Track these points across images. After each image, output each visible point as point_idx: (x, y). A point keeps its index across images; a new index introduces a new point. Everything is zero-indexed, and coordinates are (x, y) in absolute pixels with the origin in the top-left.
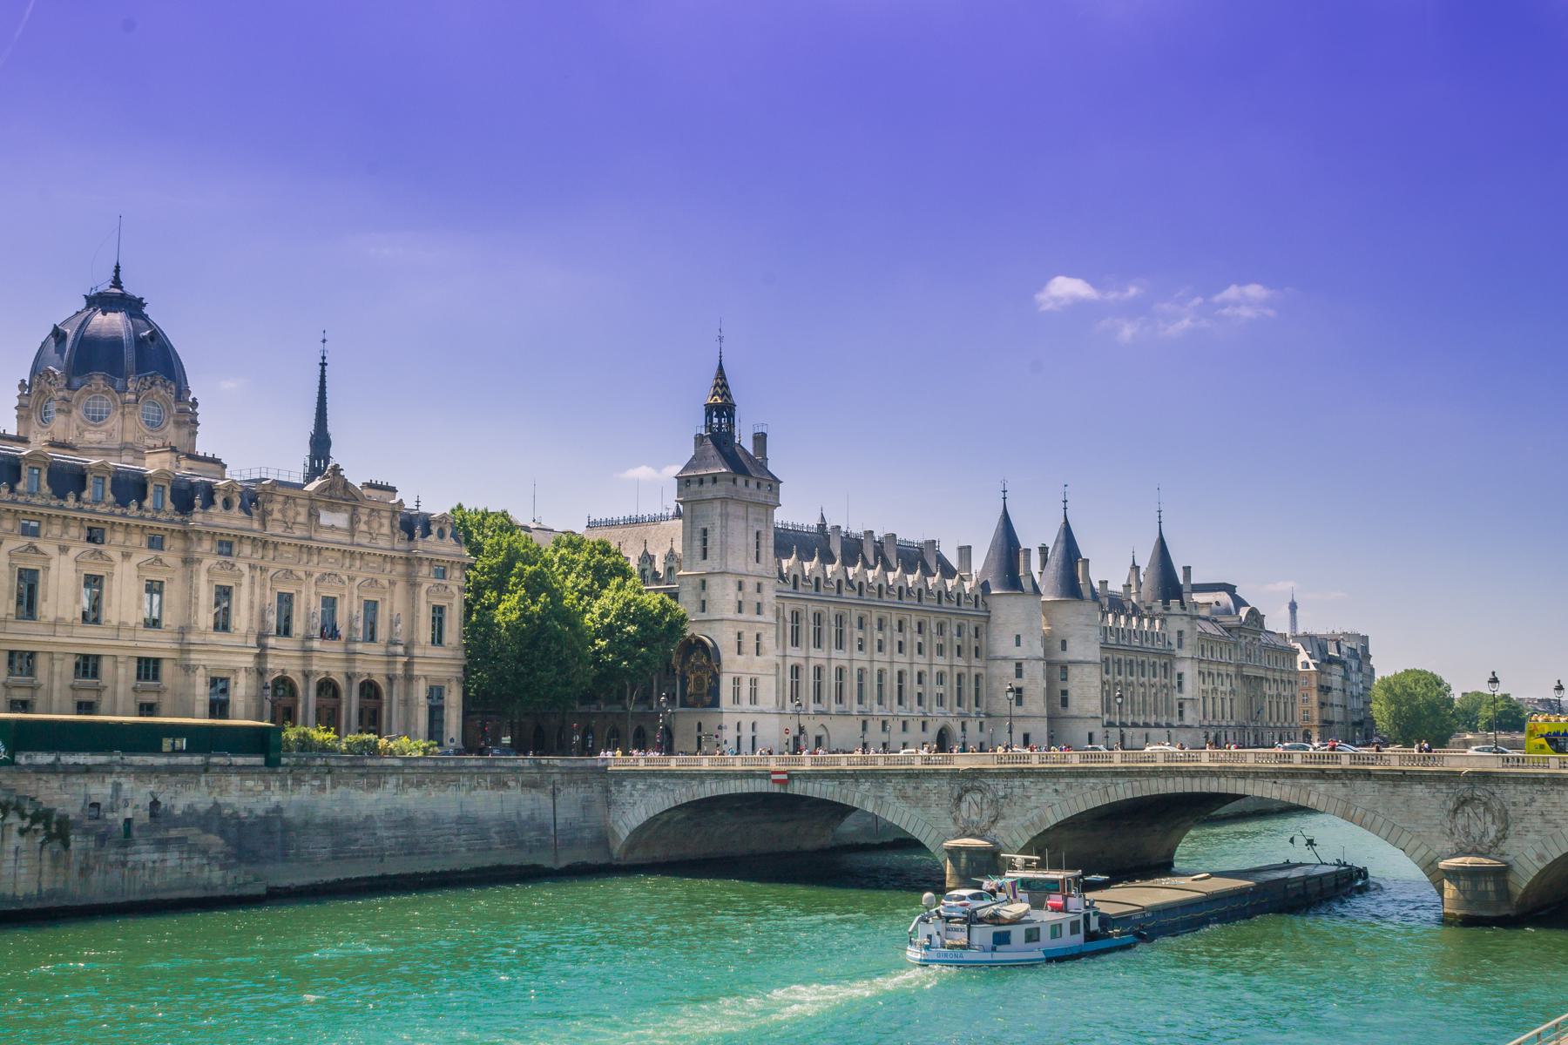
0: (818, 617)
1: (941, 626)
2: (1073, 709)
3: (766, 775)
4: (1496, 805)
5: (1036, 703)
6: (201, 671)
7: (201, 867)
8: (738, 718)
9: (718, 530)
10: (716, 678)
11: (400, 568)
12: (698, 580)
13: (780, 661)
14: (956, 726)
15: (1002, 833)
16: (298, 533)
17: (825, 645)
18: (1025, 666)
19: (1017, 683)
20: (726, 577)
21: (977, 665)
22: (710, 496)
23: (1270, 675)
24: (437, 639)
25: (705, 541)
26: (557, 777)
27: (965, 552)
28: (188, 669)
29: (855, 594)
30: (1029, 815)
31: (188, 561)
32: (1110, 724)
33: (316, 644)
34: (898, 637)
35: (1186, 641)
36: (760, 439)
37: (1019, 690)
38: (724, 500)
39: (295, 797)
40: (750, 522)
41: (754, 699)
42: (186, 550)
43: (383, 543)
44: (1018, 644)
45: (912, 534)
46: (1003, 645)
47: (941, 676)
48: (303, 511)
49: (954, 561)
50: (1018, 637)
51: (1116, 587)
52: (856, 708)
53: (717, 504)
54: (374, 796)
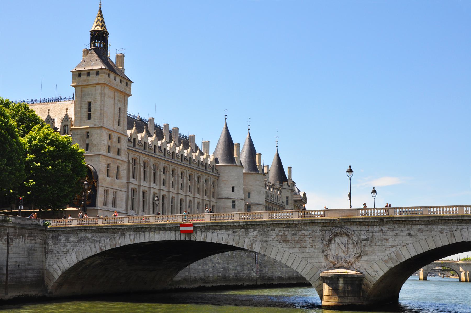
1: (199, 178)
3: (175, 228)
9: (98, 103)
12: (84, 132)
13: (126, 184)
15: (365, 266)
17: (148, 179)
18: (236, 202)
20: (103, 130)
22: (94, 82)
25: (89, 110)
26: (11, 230)
29: (162, 155)
30: (387, 252)
34: (181, 182)
36: (121, 58)
38: (103, 85)
40: (116, 102)
41: (114, 205)
44: (233, 191)
45: (185, 132)
46: (226, 191)
47: (198, 203)
50: (233, 188)
53: (99, 87)
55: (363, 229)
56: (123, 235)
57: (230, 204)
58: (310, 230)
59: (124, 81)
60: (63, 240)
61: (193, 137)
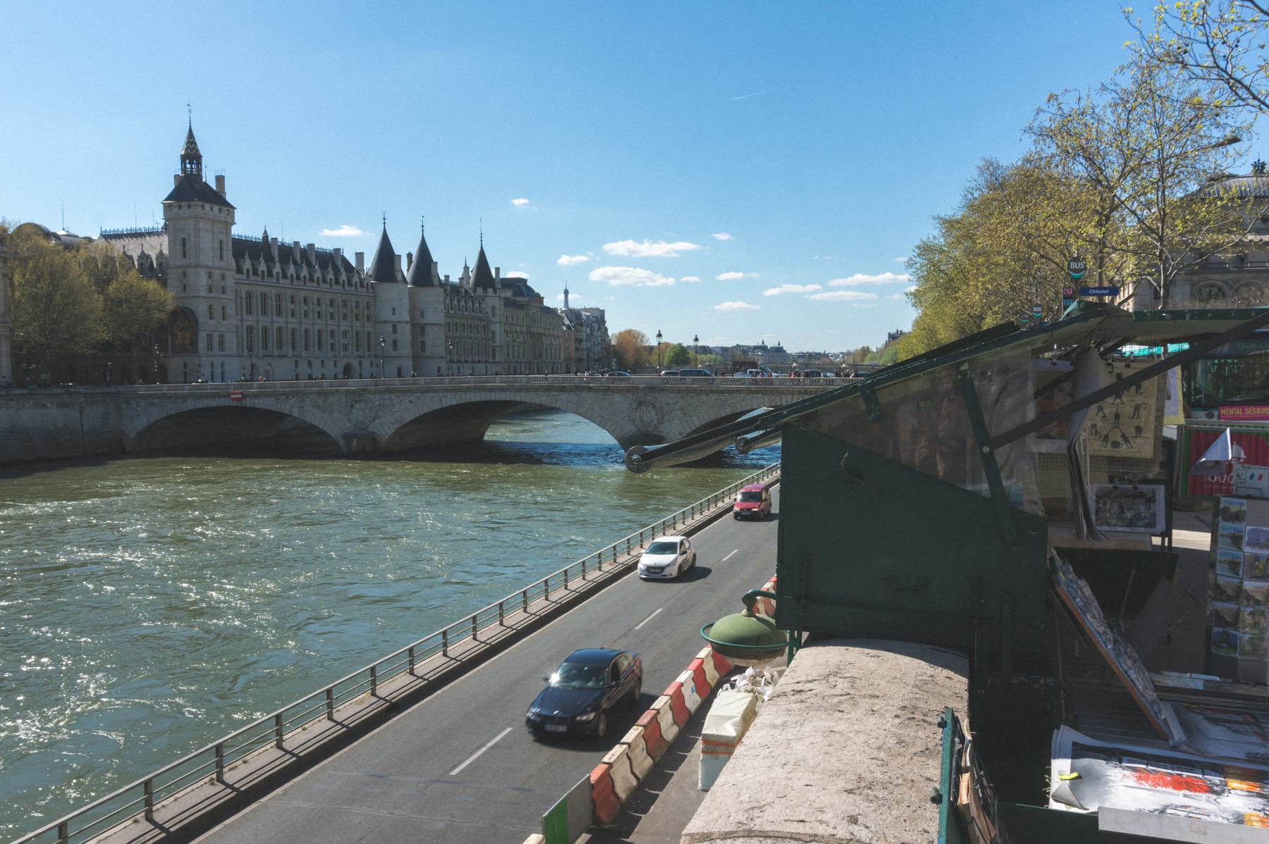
0: (264, 296)
2: (428, 353)
4: (658, 405)
14: (355, 363)
18: (398, 326)
20: (200, 270)
21: (369, 327)
23: (547, 332)
27: (360, 256)
29: (288, 281)
32: (451, 361)
34: (317, 309)
35: (497, 312)
36: (220, 180)
37: (395, 342)
38: (196, 219)
41: (222, 346)
46: (386, 315)
49: (353, 263)
51: (455, 279)
52: (290, 353)
59: (224, 209)
61: (338, 250)
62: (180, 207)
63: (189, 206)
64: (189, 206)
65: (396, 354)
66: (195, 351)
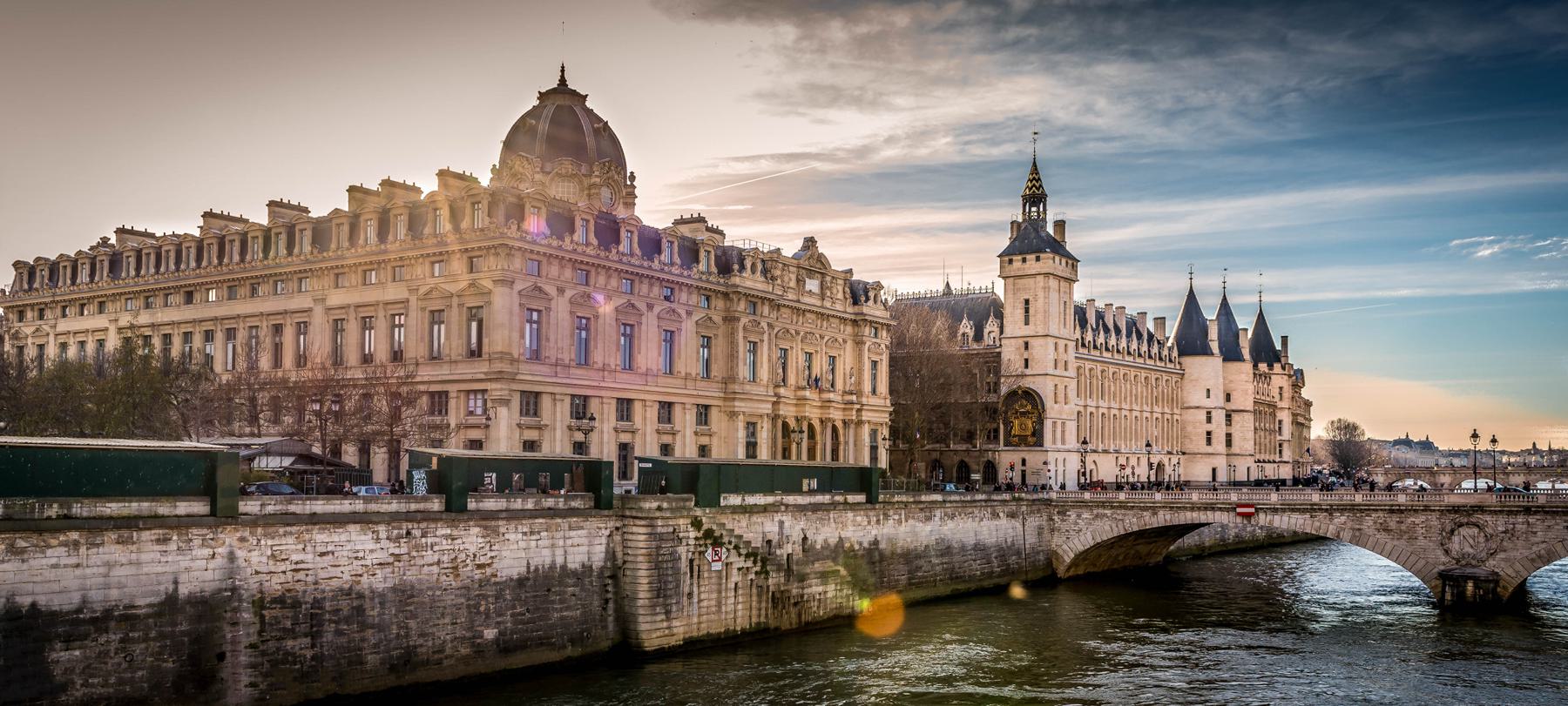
5: (1219, 445)
6: (741, 417)
7: (848, 596)
8: (1057, 455)
10: (1040, 421)
11: (849, 329)
12: (1021, 341)
16: (791, 296)
19: (1209, 427)
24: (874, 392)
25: (1027, 311)
27: (1160, 321)
28: (733, 415)
30: (1535, 548)
31: (730, 319)
33: (807, 393)
37: (1209, 433)
38: (1047, 275)
39: (885, 531)
41: (1063, 442)
42: (727, 310)
43: (839, 307)
46: (1196, 397)
48: (793, 277)
54: (928, 528)
55: (1501, 520)
56: (1155, 514)
57: (1204, 417)
58: (1423, 518)
60: (1073, 516)
62: (1024, 260)
63: (1038, 259)
64: (1038, 259)
65: (1210, 449)
66: (1039, 443)
